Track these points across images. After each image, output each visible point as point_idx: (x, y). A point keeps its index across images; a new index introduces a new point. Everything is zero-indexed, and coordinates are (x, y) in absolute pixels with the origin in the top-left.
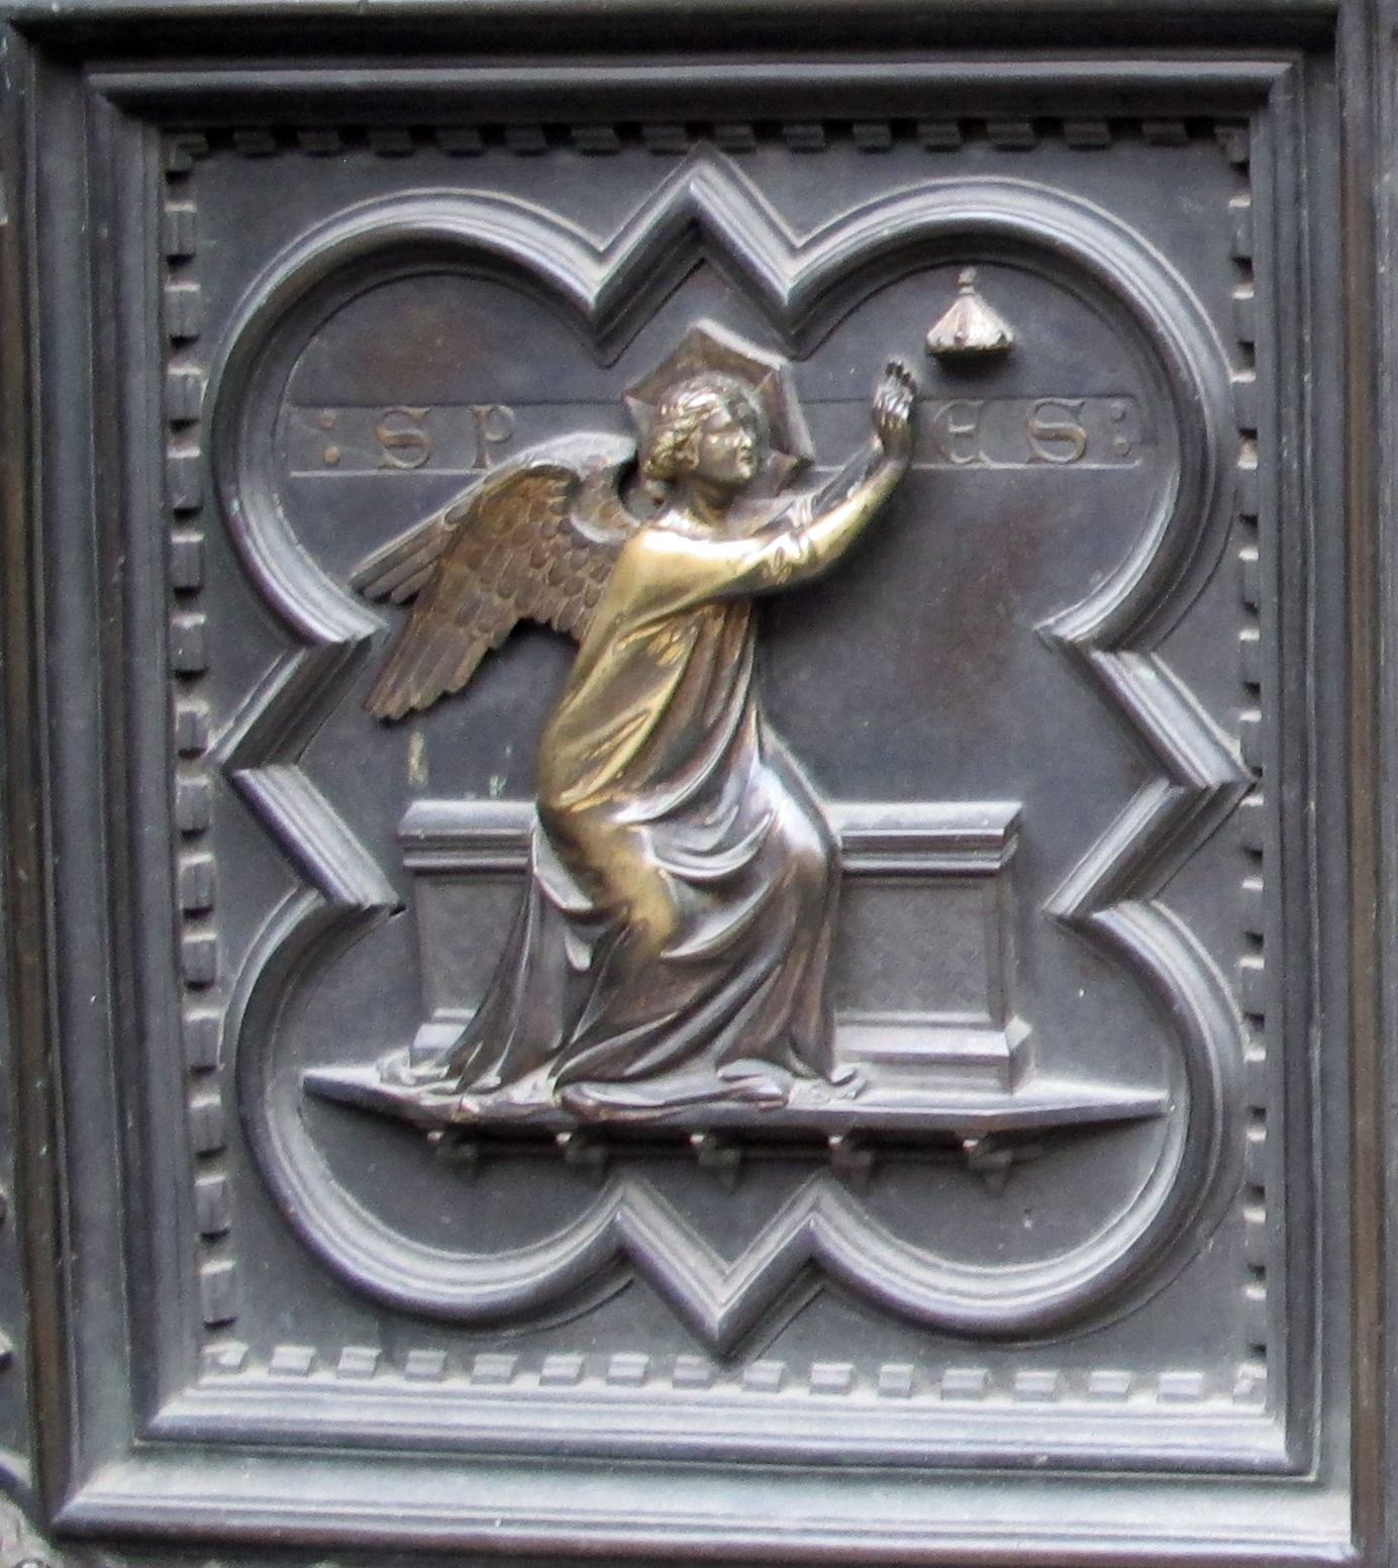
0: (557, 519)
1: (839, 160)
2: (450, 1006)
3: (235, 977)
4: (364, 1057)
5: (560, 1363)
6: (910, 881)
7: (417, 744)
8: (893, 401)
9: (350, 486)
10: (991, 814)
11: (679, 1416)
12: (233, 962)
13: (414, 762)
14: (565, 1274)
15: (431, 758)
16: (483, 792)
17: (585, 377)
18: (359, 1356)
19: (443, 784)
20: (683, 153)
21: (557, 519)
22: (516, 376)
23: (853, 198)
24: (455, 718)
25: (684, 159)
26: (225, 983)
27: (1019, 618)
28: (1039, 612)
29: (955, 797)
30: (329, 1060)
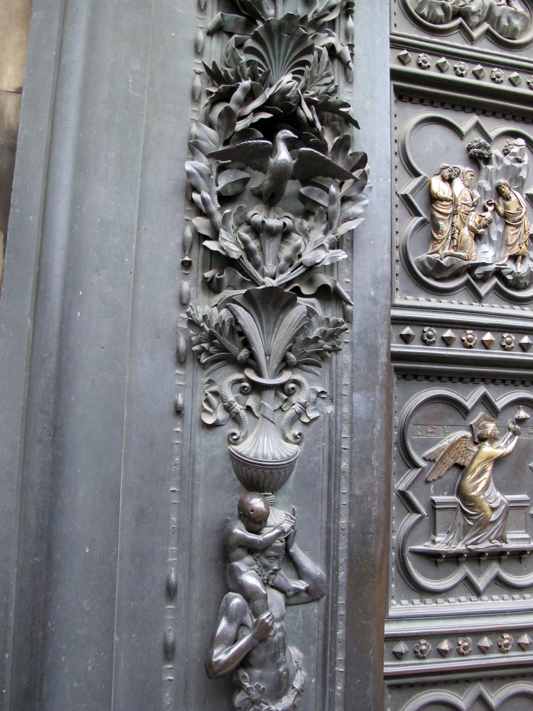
0: (464, 445)
1: (502, 387)
2: (440, 533)
3: (398, 531)
4: (420, 544)
5: (451, 599)
6: (517, 508)
7: (432, 486)
8: (511, 426)
9: (422, 439)
10: (524, 497)
11: (476, 607)
12: (398, 528)
13: (431, 489)
14: (457, 583)
15: (435, 489)
16: (443, 495)
17: (462, 422)
18: (417, 601)
19: (436, 494)
20: (479, 384)
21: (464, 445)
22: (450, 421)
23: (504, 393)
24: (440, 481)
25: (479, 385)
26: (396, 532)
27: (527, 463)
28: (529, 463)
29: (517, 494)
30: (414, 545)
